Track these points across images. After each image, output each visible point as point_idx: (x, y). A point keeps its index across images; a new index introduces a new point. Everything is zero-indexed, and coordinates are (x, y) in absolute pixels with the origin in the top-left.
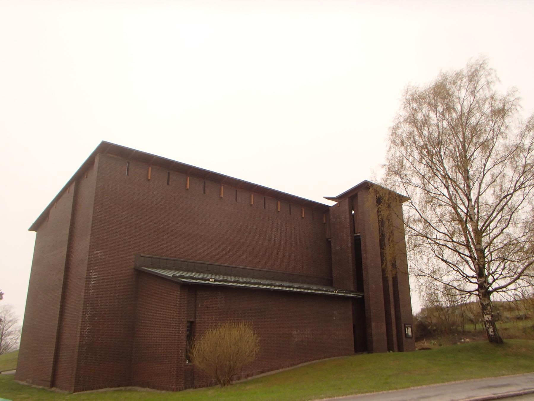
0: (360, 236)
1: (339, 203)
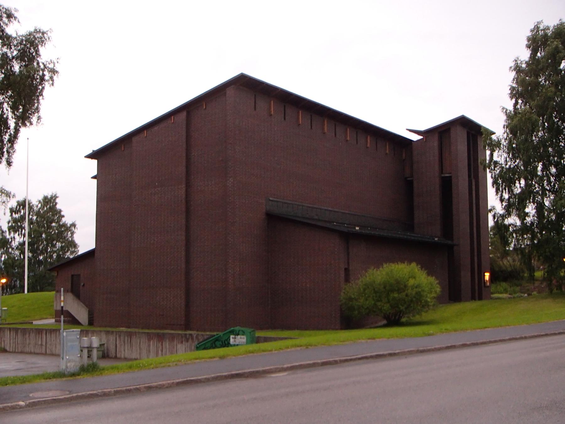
0: (451, 177)
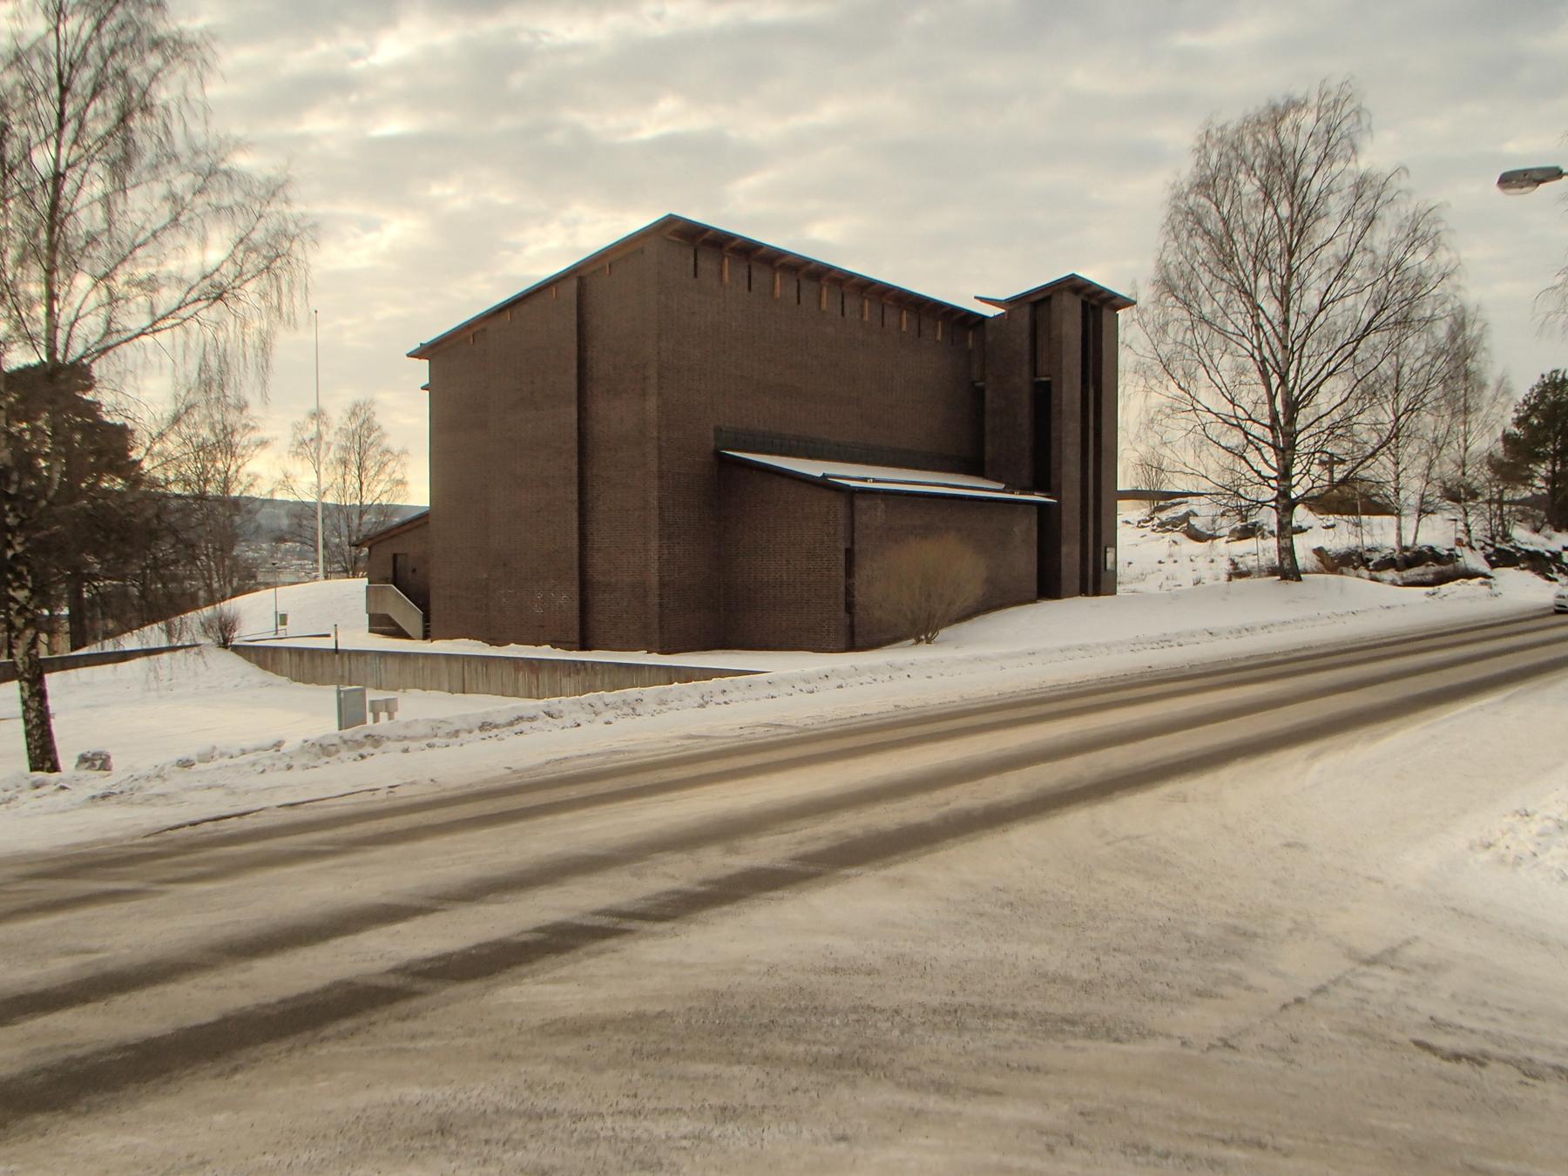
1: (1009, 312)
